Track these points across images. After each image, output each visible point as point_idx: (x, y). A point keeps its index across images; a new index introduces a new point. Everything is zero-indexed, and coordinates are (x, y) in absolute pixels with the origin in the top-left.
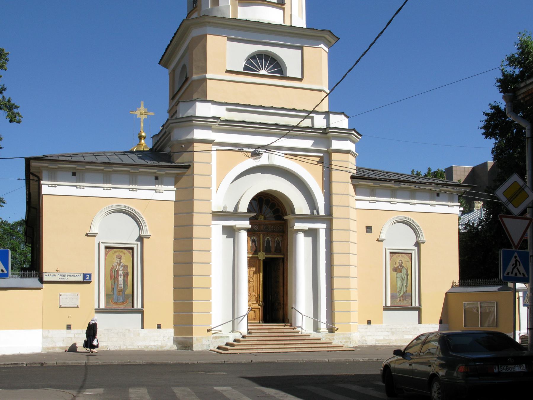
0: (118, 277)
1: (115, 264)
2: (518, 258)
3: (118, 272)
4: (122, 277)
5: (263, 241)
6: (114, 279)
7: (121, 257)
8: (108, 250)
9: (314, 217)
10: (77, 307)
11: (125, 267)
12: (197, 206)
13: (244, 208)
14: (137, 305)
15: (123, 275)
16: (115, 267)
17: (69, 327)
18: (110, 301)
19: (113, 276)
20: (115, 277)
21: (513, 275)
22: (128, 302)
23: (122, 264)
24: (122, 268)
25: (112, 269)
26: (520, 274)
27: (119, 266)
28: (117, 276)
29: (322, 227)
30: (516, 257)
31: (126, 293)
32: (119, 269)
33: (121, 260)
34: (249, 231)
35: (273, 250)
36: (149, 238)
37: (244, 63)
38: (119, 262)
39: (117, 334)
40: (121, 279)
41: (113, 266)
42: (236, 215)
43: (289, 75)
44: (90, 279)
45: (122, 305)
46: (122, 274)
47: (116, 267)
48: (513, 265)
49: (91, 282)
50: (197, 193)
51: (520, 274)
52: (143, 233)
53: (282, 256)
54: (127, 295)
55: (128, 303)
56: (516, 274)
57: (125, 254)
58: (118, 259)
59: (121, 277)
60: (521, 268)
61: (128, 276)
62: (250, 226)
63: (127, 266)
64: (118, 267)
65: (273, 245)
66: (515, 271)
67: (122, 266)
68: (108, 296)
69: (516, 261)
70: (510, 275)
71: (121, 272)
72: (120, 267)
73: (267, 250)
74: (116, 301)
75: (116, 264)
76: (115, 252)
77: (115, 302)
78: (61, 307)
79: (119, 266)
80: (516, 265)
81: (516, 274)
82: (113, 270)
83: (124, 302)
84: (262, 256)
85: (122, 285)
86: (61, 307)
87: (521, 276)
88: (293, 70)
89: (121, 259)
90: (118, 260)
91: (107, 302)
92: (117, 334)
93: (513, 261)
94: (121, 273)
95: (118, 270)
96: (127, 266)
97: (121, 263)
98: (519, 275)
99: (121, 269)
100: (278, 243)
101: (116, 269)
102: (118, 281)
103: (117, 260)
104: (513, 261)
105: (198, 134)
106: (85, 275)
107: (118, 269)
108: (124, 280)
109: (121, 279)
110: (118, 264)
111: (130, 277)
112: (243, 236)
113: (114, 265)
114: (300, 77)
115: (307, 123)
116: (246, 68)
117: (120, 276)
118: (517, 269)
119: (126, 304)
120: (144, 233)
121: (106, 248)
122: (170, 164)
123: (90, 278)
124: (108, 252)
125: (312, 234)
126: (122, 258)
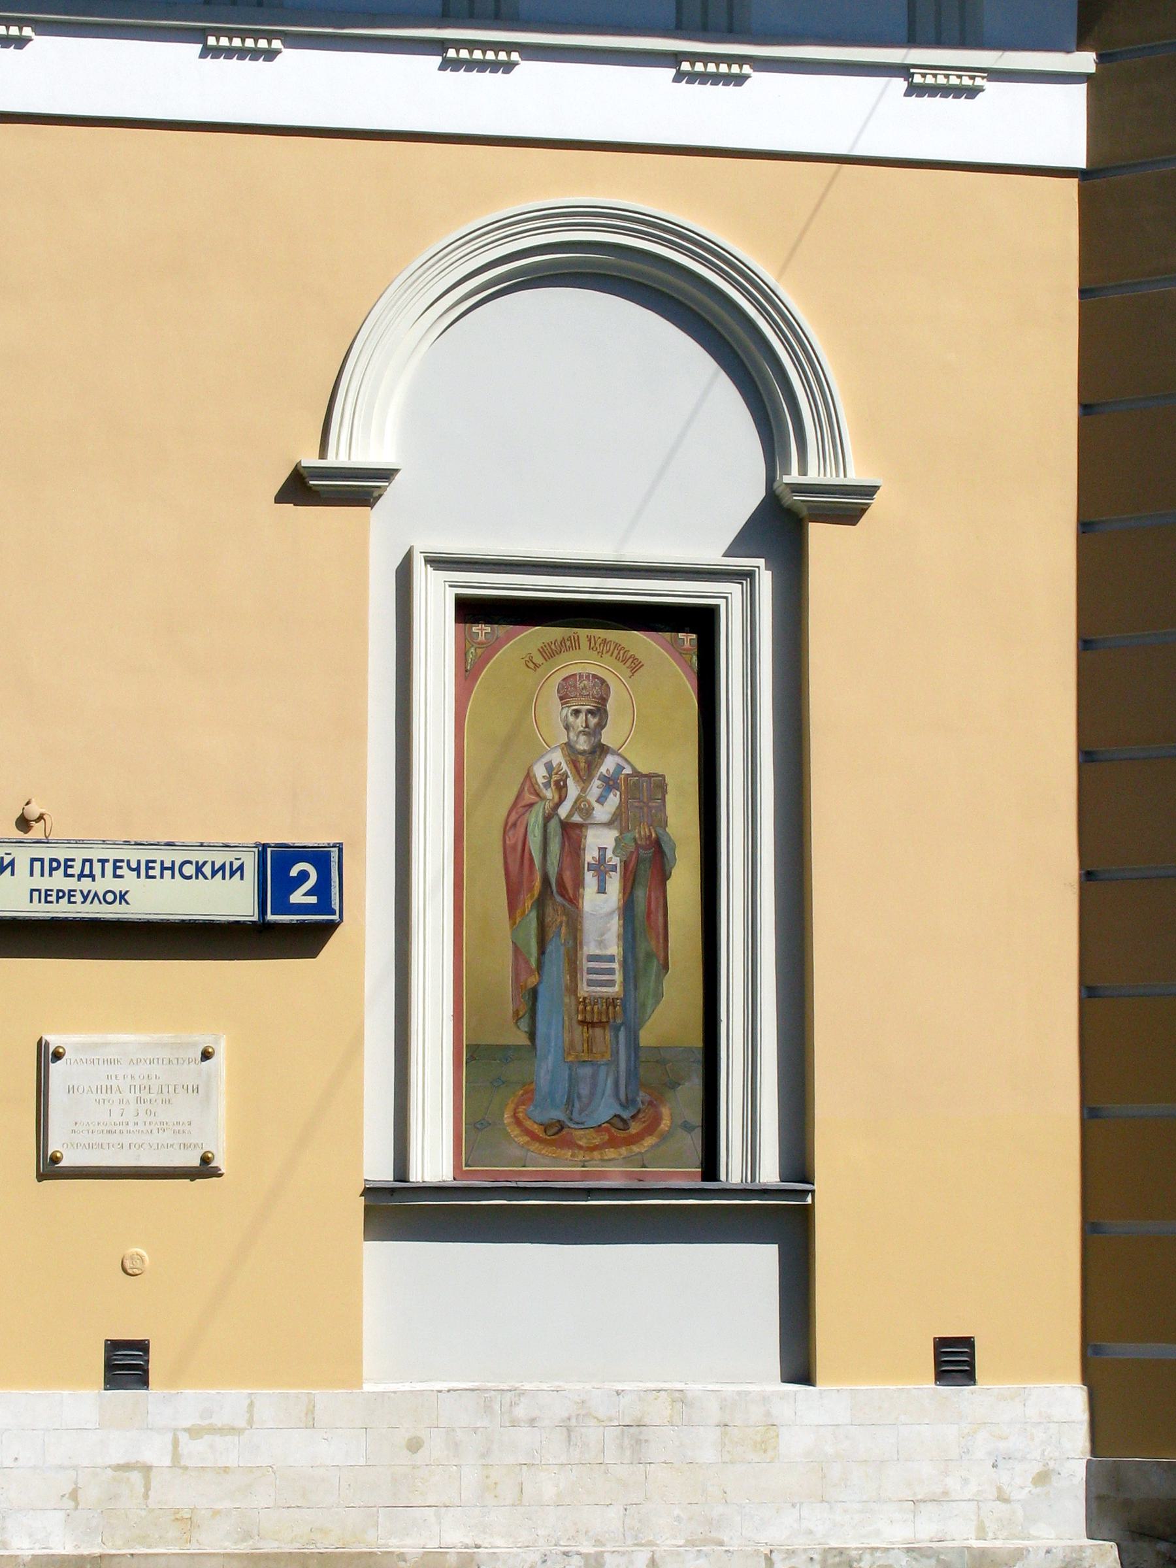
0: (579, 883)
1: (549, 766)
3: (572, 833)
4: (614, 884)
6: (540, 904)
7: (603, 700)
8: (481, 630)
15: (626, 864)
16: (549, 794)
18: (507, 1117)
20: (546, 880)
22: (665, 1124)
23: (609, 764)
24: (614, 800)
25: (520, 807)
27: (585, 778)
28: (568, 876)
31: (647, 1037)
32: (585, 810)
33: (601, 725)
36: (849, 515)
38: (583, 744)
39: (568, 1428)
41: (529, 776)
44: (324, 906)
45: (610, 1153)
46: (616, 861)
47: (561, 788)
49: (331, 927)
52: (803, 471)
54: (660, 1057)
55: (664, 1138)
57: (635, 665)
58: (577, 713)
59: (602, 890)
61: (663, 876)
63: (658, 784)
64: (573, 790)
67: (610, 783)
72: (595, 788)
74: (557, 1114)
75: (557, 758)
76: (550, 652)
77: (546, 1127)
79: (585, 778)
82: (535, 820)
83: (635, 1128)
85: (611, 959)
89: (600, 711)
90: (580, 722)
92: (568, 1428)
94: (602, 850)
95: (577, 818)
96: (658, 784)
97: (600, 750)
99: (602, 813)
101: (563, 812)
103: (567, 727)
107: (576, 807)
108: (628, 909)
110: (574, 764)
113: (540, 772)
117: (590, 879)
119: (649, 1141)
123: (322, 889)
124: (490, 649)
126: (609, 706)
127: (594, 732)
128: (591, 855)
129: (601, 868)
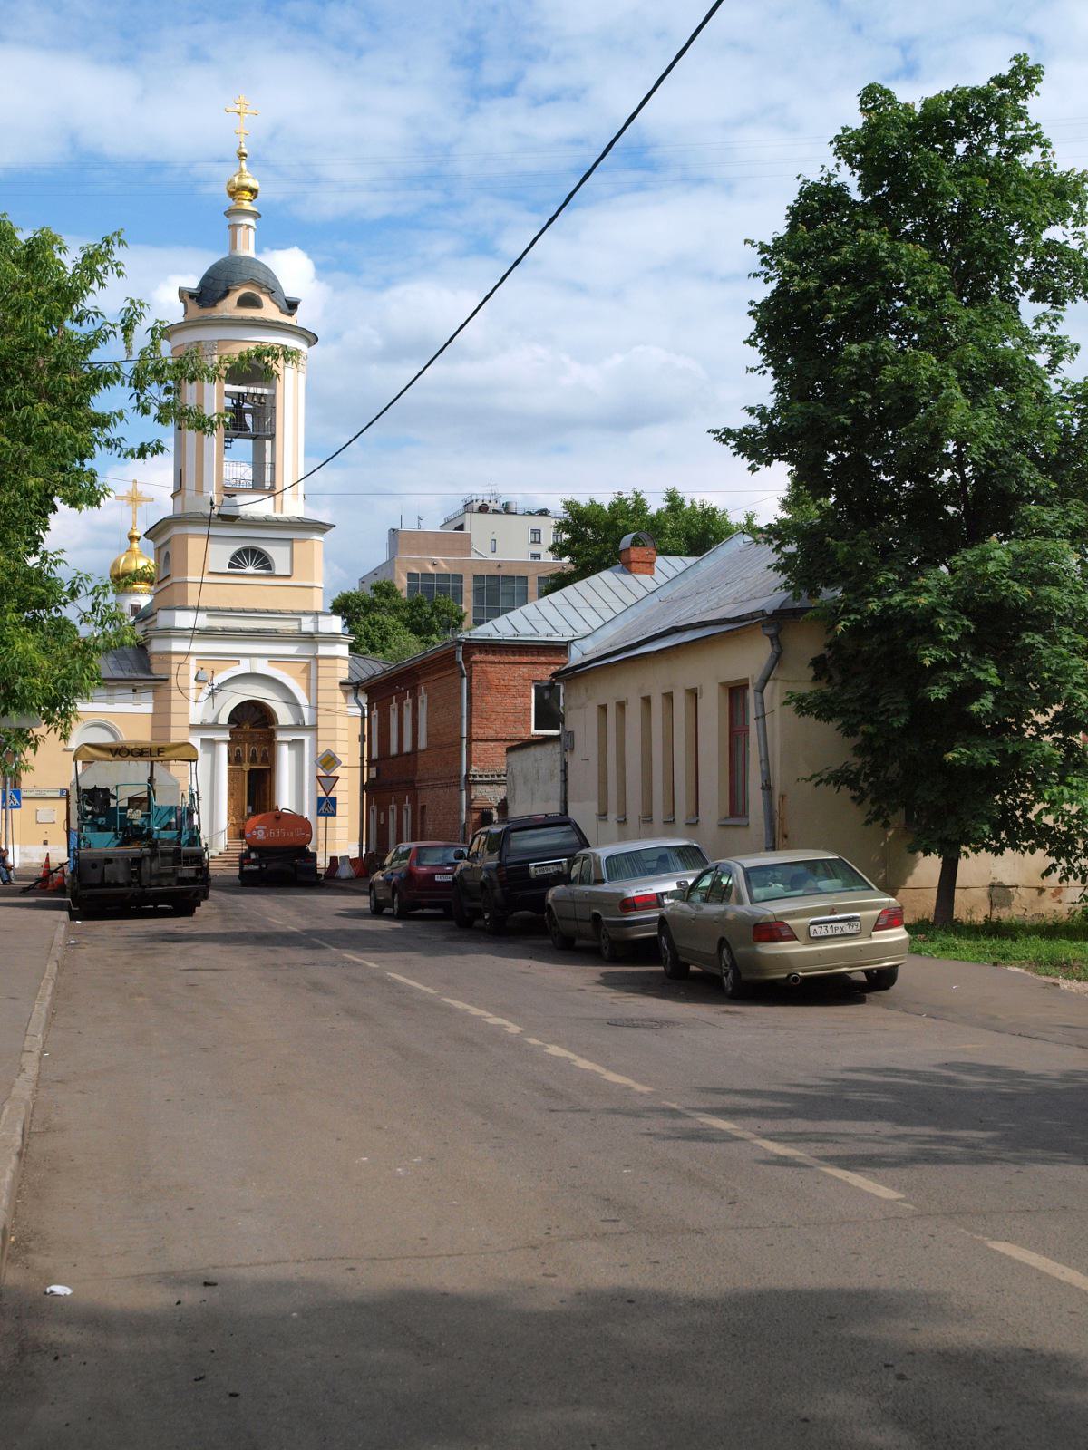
5: (249, 751)
9: (299, 727)
10: (54, 823)
12: (175, 720)
13: (224, 720)
17: (45, 843)
29: (306, 737)
34: (229, 743)
35: (259, 760)
37: (229, 561)
42: (214, 726)
43: (276, 573)
50: (175, 707)
53: (269, 767)
62: (229, 739)
65: (259, 755)
73: (253, 760)
78: (38, 822)
84: (247, 767)
86: (38, 822)
88: (281, 566)
93: (325, 803)
100: (265, 753)
104: (325, 803)
105: (177, 646)
112: (224, 749)
114: (288, 573)
115: (292, 626)
122: (149, 677)
125: (296, 744)
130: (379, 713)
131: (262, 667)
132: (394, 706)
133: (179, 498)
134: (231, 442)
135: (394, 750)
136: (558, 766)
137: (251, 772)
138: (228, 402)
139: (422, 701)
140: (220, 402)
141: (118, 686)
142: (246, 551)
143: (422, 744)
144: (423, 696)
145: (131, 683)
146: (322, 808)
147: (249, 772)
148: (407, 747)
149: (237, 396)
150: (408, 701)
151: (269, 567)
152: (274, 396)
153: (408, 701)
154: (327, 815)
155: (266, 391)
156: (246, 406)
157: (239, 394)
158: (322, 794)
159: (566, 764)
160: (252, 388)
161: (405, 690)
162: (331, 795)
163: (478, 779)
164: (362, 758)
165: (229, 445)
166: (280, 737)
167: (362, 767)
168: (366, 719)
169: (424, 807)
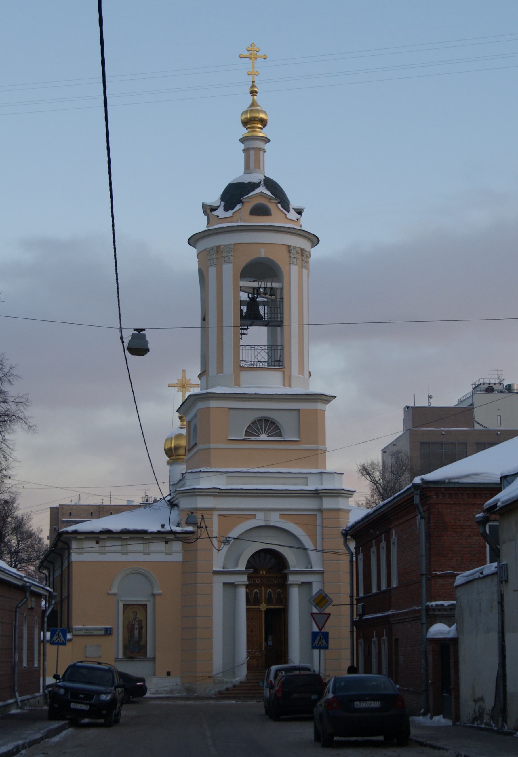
2: (322, 636)
3: (134, 625)
5: (265, 593)
11: (140, 622)
14: (149, 654)
19: (129, 629)
21: (319, 645)
23: (137, 619)
26: (323, 644)
30: (320, 636)
38: (135, 617)
40: (136, 632)
47: (133, 621)
48: (319, 640)
51: (323, 644)
56: (320, 645)
60: (324, 642)
64: (134, 621)
66: (320, 643)
67: (137, 621)
68: (125, 647)
69: (320, 638)
70: (317, 645)
71: (136, 626)
72: (136, 621)
73: (269, 601)
75: (132, 618)
79: (135, 620)
80: (320, 640)
81: (320, 645)
84: (263, 607)
87: (324, 646)
89: (136, 614)
91: (124, 653)
93: (318, 638)
97: (136, 618)
98: (322, 645)
99: (137, 623)
101: (133, 623)
102: (134, 634)
106: (106, 630)
108: (139, 632)
109: (136, 632)
111: (144, 630)
113: (131, 620)
116: (247, 433)
118: (321, 642)
120: (156, 591)
121: (124, 605)
123: (110, 631)
127: (136, 616)
128: (135, 627)
129: (136, 629)
130: (364, 556)
131: (275, 520)
132: (374, 549)
133: (204, 378)
134: (247, 329)
135: (374, 590)
136: (496, 597)
137: (268, 612)
138: (244, 296)
139: (394, 543)
140: (236, 296)
141: (131, 539)
142: (260, 420)
143: (394, 585)
144: (394, 538)
145: (164, 536)
146: (316, 642)
147: (265, 612)
148: (384, 587)
149: (251, 291)
150: (383, 544)
151: (280, 434)
152: (282, 289)
153: (383, 544)
154: (320, 648)
155: (276, 285)
156: (259, 299)
157: (254, 288)
158: (316, 629)
159: (502, 596)
160: (263, 283)
161: (381, 535)
162: (323, 631)
163: (437, 613)
164: (352, 597)
165: (245, 332)
166: (292, 579)
167: (352, 605)
168: (354, 563)
169: (397, 640)
